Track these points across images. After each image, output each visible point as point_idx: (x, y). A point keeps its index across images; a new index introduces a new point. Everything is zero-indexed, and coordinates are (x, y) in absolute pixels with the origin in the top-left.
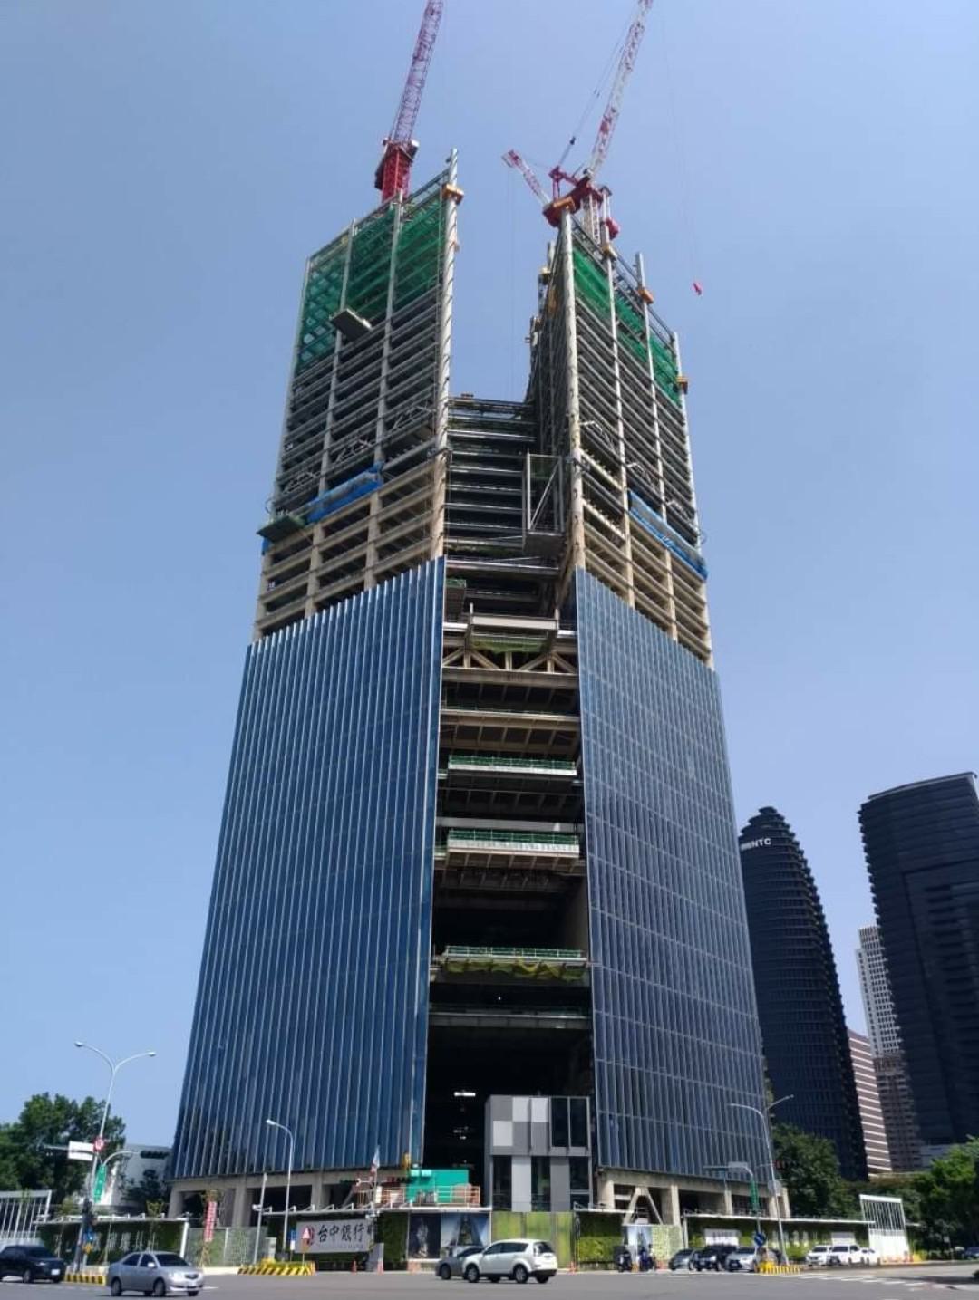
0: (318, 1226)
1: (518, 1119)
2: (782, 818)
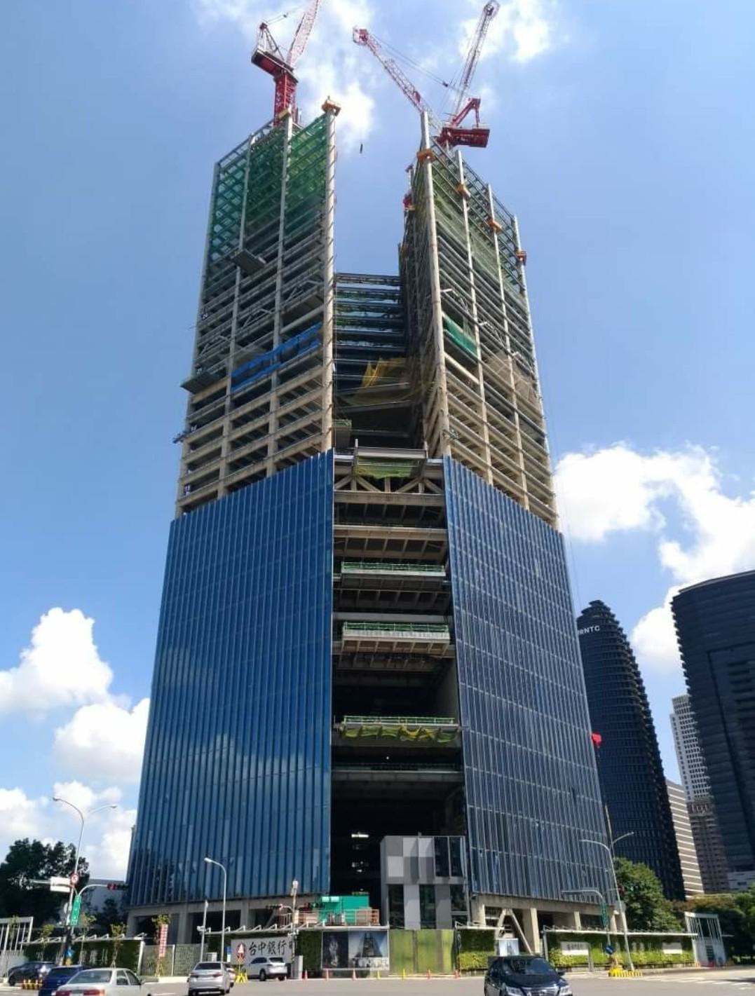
0: (248, 942)
1: (405, 856)
2: (609, 609)
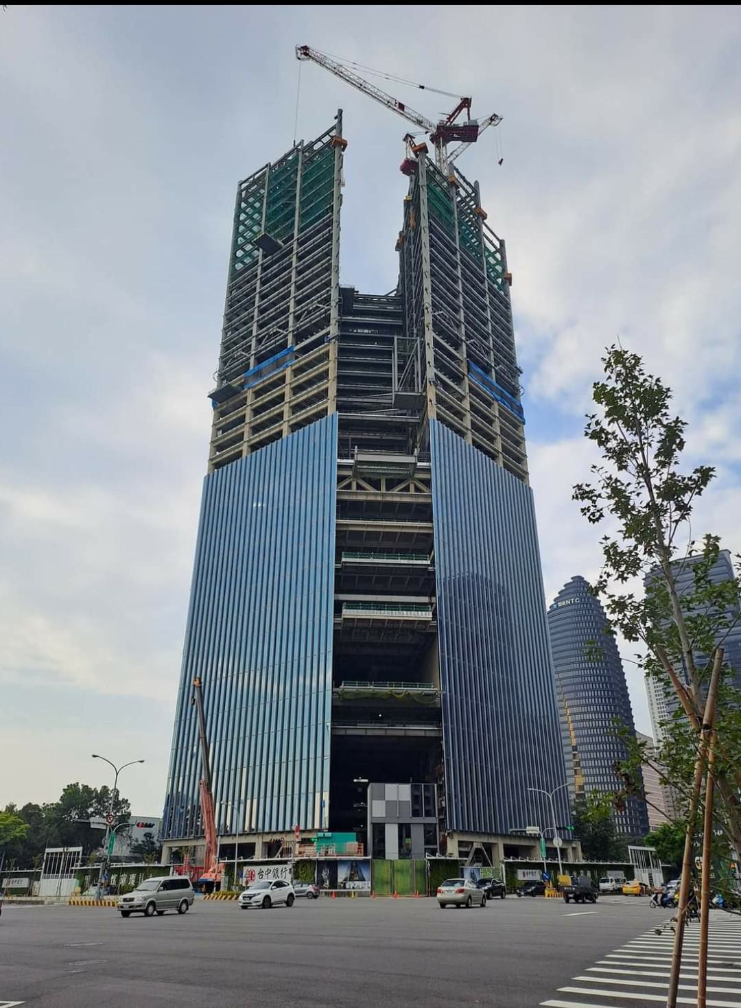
1: (388, 800)
